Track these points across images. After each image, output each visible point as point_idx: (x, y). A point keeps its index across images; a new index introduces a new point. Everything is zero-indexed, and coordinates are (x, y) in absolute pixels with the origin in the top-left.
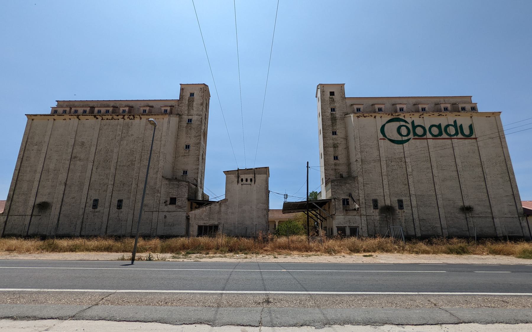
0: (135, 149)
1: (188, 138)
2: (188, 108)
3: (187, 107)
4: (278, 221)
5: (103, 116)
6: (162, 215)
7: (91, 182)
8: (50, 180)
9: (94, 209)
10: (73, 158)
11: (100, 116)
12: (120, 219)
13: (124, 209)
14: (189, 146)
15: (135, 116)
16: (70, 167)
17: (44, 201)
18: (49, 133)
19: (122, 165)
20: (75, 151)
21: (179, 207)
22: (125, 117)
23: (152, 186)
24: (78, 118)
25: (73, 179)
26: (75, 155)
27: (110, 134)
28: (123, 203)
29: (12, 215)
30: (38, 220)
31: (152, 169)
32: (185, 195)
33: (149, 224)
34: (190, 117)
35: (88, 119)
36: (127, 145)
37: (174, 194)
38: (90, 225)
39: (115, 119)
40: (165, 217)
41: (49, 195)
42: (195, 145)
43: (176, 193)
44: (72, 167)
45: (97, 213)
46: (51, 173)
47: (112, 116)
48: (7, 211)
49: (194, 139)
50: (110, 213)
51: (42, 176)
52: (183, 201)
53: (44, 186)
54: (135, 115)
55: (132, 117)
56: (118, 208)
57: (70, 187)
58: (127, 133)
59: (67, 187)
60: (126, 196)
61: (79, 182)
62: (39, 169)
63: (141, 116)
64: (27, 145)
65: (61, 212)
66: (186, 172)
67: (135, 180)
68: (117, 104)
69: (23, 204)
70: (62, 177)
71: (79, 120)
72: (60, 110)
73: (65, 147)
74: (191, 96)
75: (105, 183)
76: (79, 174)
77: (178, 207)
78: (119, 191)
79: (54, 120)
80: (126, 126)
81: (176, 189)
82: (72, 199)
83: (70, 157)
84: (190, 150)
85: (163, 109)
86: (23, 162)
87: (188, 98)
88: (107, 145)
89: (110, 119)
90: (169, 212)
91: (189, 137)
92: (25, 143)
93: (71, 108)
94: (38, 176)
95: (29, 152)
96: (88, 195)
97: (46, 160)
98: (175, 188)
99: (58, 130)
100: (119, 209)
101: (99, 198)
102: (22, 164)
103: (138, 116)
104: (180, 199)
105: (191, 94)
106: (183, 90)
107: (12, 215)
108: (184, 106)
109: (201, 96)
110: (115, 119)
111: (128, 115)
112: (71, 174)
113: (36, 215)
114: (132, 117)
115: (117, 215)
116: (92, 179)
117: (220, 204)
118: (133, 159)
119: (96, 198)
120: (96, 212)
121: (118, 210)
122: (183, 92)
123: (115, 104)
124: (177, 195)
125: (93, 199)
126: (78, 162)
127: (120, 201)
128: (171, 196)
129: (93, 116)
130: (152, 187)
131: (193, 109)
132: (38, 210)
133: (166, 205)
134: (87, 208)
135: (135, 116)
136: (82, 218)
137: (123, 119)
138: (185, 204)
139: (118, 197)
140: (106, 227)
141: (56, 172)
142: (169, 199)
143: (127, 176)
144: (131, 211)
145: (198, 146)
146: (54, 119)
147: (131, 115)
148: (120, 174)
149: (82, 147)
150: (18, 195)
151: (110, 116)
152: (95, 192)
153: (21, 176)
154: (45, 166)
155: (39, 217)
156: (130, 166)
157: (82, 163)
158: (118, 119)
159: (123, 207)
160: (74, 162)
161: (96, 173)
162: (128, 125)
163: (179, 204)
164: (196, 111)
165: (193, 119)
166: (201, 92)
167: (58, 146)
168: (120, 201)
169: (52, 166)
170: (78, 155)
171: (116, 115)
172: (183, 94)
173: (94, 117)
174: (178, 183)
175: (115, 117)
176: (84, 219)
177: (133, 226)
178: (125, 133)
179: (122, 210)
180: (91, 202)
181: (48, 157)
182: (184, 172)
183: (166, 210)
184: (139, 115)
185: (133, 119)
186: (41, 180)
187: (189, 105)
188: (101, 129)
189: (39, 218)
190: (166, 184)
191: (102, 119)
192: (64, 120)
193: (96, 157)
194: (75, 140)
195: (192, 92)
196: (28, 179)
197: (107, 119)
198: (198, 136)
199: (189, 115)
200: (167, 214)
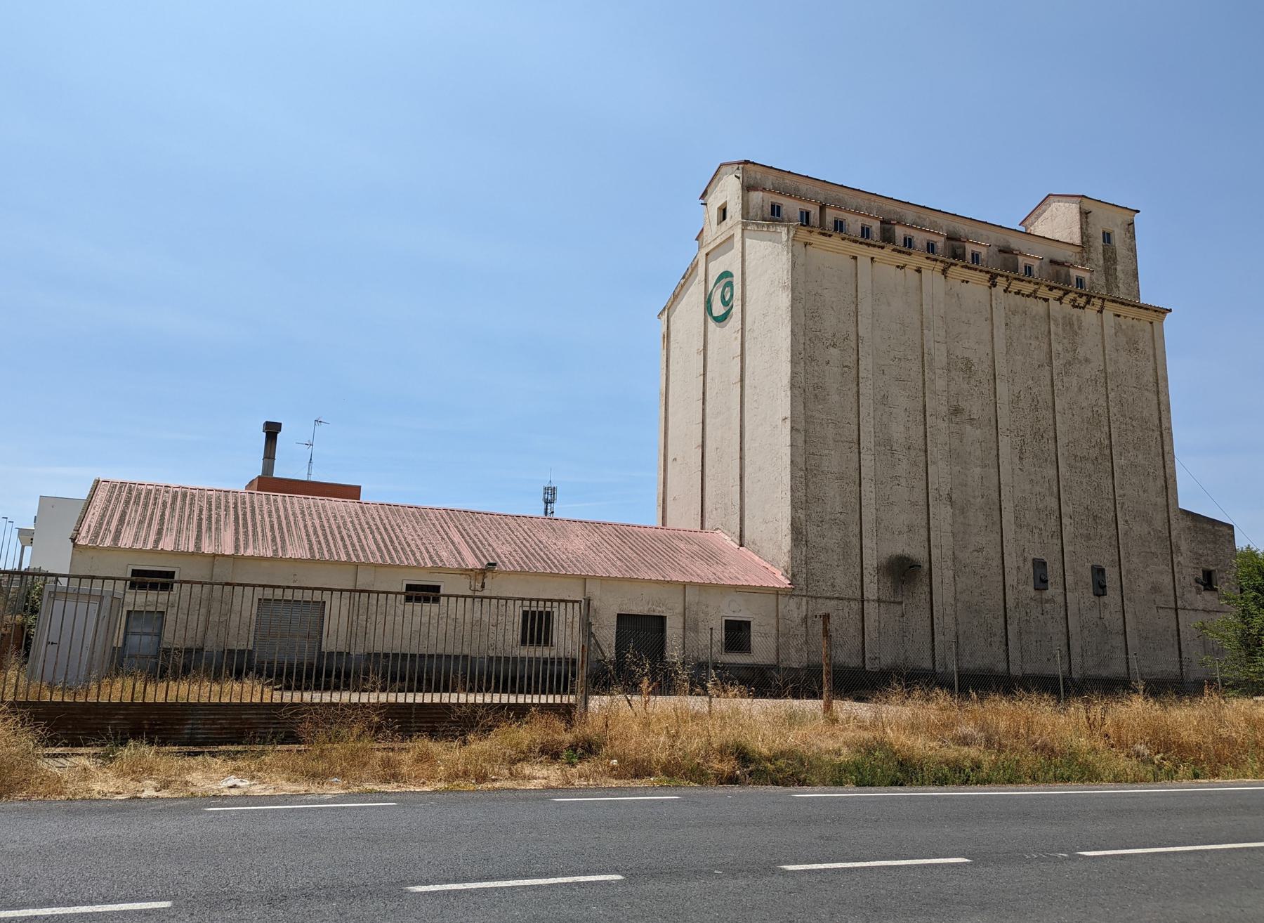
2: (1107, 280)
5: (1014, 282)
9: (1038, 592)
11: (1007, 280)
12: (1106, 628)
13: (1112, 596)
15: (1093, 300)
17: (899, 552)
22: (1066, 296)
23: (1160, 531)
24: (944, 272)
25: (966, 485)
30: (897, 618)
33: (1173, 646)
38: (1039, 643)
39: (1036, 298)
45: (1047, 605)
46: (901, 457)
47: (1036, 287)
53: (890, 501)
55: (1082, 301)
56: (1101, 592)
60: (1107, 556)
67: (1122, 508)
68: (925, 220)
69: (841, 557)
75: (1049, 508)
78: (1088, 538)
80: (1068, 328)
81: (1211, 546)
88: (1030, 382)
89: (1023, 295)
95: (816, 368)
99: (889, 304)
100: (1099, 596)
101: (1043, 557)
111: (1076, 293)
113: (891, 602)
114: (1082, 301)
115: (1096, 613)
118: (1102, 439)
120: (1047, 601)
123: (919, 217)
124: (1216, 565)
125: (1030, 558)
126: (968, 427)
127: (1098, 572)
130: (1160, 534)
132: (889, 584)
135: (1093, 300)
137: (1058, 302)
141: (913, 453)
148: (1081, 482)
149: (969, 377)
150: (818, 526)
153: (813, 454)
155: (898, 608)
156: (1100, 461)
157: (979, 431)
158: (1046, 300)
161: (1020, 472)
166: (1128, 235)
167: (900, 359)
168: (1098, 572)
169: (897, 432)
170: (962, 405)
174: (1213, 527)
175: (1044, 291)
185: (1080, 308)
189: (900, 612)
190: (1189, 528)
192: (898, 267)
195: (1108, 229)
196: (836, 470)
197: (1018, 293)
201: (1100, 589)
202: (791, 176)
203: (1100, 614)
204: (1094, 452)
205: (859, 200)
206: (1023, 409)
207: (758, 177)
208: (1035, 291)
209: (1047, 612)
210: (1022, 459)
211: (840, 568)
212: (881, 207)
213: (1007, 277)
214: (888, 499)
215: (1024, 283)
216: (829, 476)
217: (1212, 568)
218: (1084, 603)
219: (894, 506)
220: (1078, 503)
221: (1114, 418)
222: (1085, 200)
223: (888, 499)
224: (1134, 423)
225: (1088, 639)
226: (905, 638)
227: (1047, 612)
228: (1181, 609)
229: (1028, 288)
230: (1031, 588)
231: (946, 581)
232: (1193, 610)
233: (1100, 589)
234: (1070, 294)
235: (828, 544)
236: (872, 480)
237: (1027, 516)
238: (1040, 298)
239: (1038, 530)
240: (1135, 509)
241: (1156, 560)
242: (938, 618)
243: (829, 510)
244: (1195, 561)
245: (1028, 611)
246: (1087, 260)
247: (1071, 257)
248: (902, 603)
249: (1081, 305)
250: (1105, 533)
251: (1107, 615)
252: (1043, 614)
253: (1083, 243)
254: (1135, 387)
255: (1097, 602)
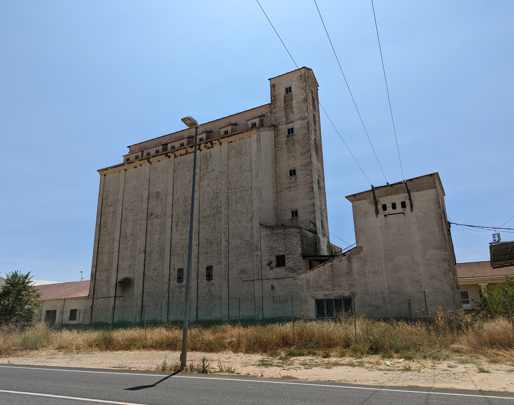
0: (219, 190)
1: (292, 159)
2: (286, 112)
3: (284, 112)
4: (487, 284)
6: (267, 285)
7: (173, 245)
8: (129, 249)
9: (179, 283)
10: (149, 215)
11: (173, 153)
12: (212, 295)
13: (216, 279)
14: (294, 171)
15: (213, 142)
16: (148, 228)
17: (125, 276)
18: (122, 188)
19: (205, 215)
20: (150, 206)
21: (291, 270)
22: (201, 147)
24: (149, 161)
26: (151, 212)
27: (187, 175)
28: (214, 270)
29: (97, 298)
30: (122, 302)
31: (244, 215)
32: (297, 250)
34: (290, 126)
35: (160, 161)
36: (208, 185)
37: (281, 249)
39: (190, 153)
40: (273, 288)
41: (130, 269)
42: (303, 167)
43: (283, 247)
44: (149, 227)
45: (183, 288)
46: (129, 239)
47: (185, 149)
48: (92, 293)
49: (301, 158)
50: (200, 286)
51: (121, 245)
52: (295, 259)
53: (124, 257)
54: (213, 141)
55: (209, 145)
57: (150, 255)
58: (207, 169)
59: (147, 255)
60: (216, 260)
61: (159, 247)
62: (117, 237)
63: (220, 140)
64: (103, 208)
65: (145, 290)
66: (296, 212)
69: (106, 282)
70: (141, 243)
71: (151, 163)
72: (132, 157)
73: (140, 203)
74: (287, 92)
76: (158, 236)
77: (290, 271)
79: (125, 170)
81: (282, 241)
82: (154, 271)
83: (146, 215)
84: (297, 177)
85: (250, 123)
86: (101, 230)
87: (283, 97)
89: (184, 155)
90: (277, 279)
91: (293, 156)
92: (101, 206)
93: (143, 152)
94: (116, 244)
95: (105, 216)
96: (171, 263)
97: (122, 223)
98: (280, 240)
100: (209, 280)
101: (183, 267)
102: (101, 233)
103: (217, 141)
104: (291, 256)
105: (287, 89)
106: (274, 88)
107: (97, 298)
108: (280, 111)
109: (303, 88)
110: (190, 153)
111: (204, 143)
112: (150, 237)
114: (209, 145)
116: (174, 241)
117: (349, 259)
119: (181, 267)
121: (208, 282)
122: (274, 89)
124: (285, 251)
126: (155, 220)
127: (209, 269)
128: (276, 254)
129: (164, 155)
130: (248, 242)
131: (293, 112)
133: (272, 268)
134: (171, 282)
135: (213, 142)
136: (167, 297)
137: (199, 150)
138: (299, 264)
139: (206, 263)
140: (196, 308)
141: (134, 237)
142: (274, 259)
143: (213, 230)
144: (224, 282)
145: (308, 168)
146: (125, 169)
147: (208, 142)
148: (205, 228)
150: (100, 272)
151: (183, 150)
152: (178, 259)
154: (122, 232)
156: (216, 215)
157: (159, 220)
159: (213, 277)
160: (151, 221)
162: (206, 157)
163: (289, 265)
164: (298, 113)
165: (295, 127)
167: (133, 202)
168: (209, 269)
171: (189, 147)
172: (276, 93)
173: (166, 155)
174: (285, 231)
176: (170, 299)
177: (230, 305)
178: (203, 170)
179: (213, 281)
180: (175, 273)
181: (123, 219)
182: (293, 212)
183: (273, 277)
184: (218, 140)
185: (211, 147)
186: (120, 250)
187: (286, 108)
188: (175, 170)
189: (123, 300)
190: (267, 235)
191: (175, 157)
192: (135, 168)
193: (174, 208)
194: (149, 191)
195: (288, 86)
197: (181, 155)
198: (306, 152)
199: (288, 122)
200: (275, 283)
201: (209, 277)
202: (143, 143)
203: (209, 289)
204: (213, 212)
205: (167, 139)
206: (180, 204)
207: (134, 149)
208: (187, 151)
209: (183, 292)
210: (178, 225)
211: (105, 286)
212: (175, 137)
213: (171, 152)
214: (123, 257)
215: (179, 151)
216: (105, 253)
217: (282, 254)
218: (202, 285)
219: (125, 259)
220: (203, 238)
221: (224, 192)
222: (272, 80)
223: (123, 257)
224: (237, 191)
225: (202, 302)
226: (124, 310)
227: (183, 292)
228: (257, 280)
229: (183, 151)
230: (176, 282)
231: (139, 285)
232: (267, 279)
233: (209, 277)
234: (201, 145)
235: (102, 278)
236: (117, 251)
237: (177, 250)
238: (191, 152)
239: (182, 255)
240: (234, 233)
241: (244, 256)
242: (135, 300)
243: (104, 266)
244: (270, 252)
245: (174, 292)
246: (274, 108)
247: (264, 111)
248: (124, 296)
249: (210, 147)
250: (215, 249)
251: (213, 289)
252: (180, 293)
253: (271, 101)
254: (239, 173)
255: (208, 283)
